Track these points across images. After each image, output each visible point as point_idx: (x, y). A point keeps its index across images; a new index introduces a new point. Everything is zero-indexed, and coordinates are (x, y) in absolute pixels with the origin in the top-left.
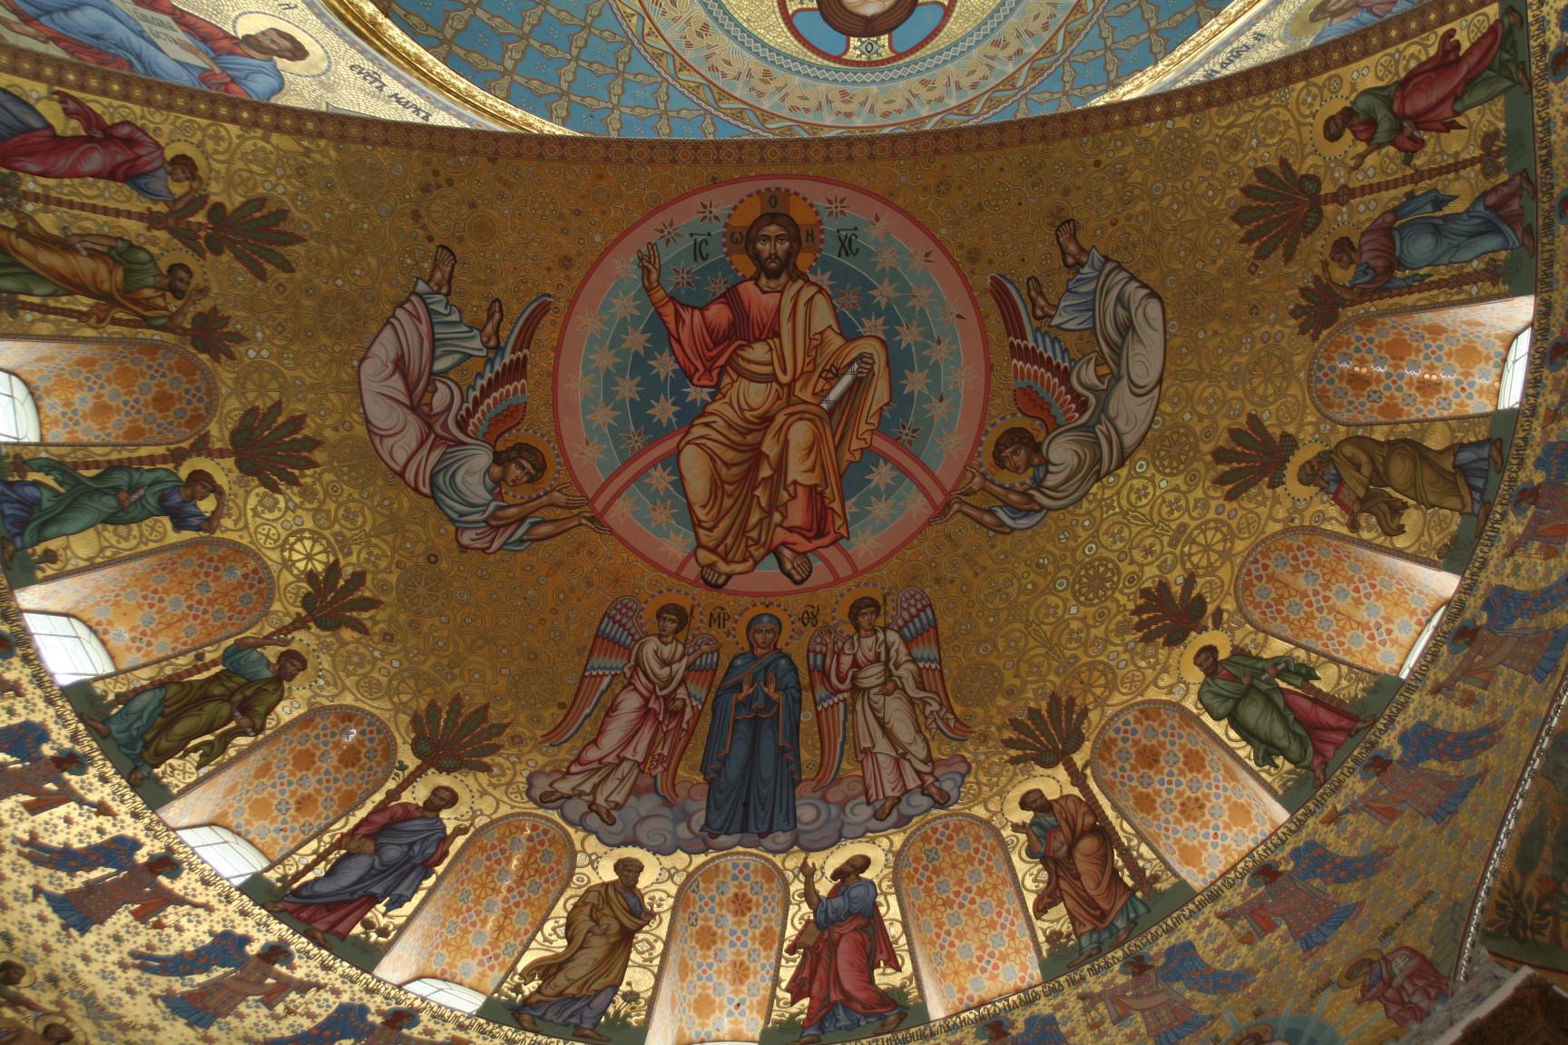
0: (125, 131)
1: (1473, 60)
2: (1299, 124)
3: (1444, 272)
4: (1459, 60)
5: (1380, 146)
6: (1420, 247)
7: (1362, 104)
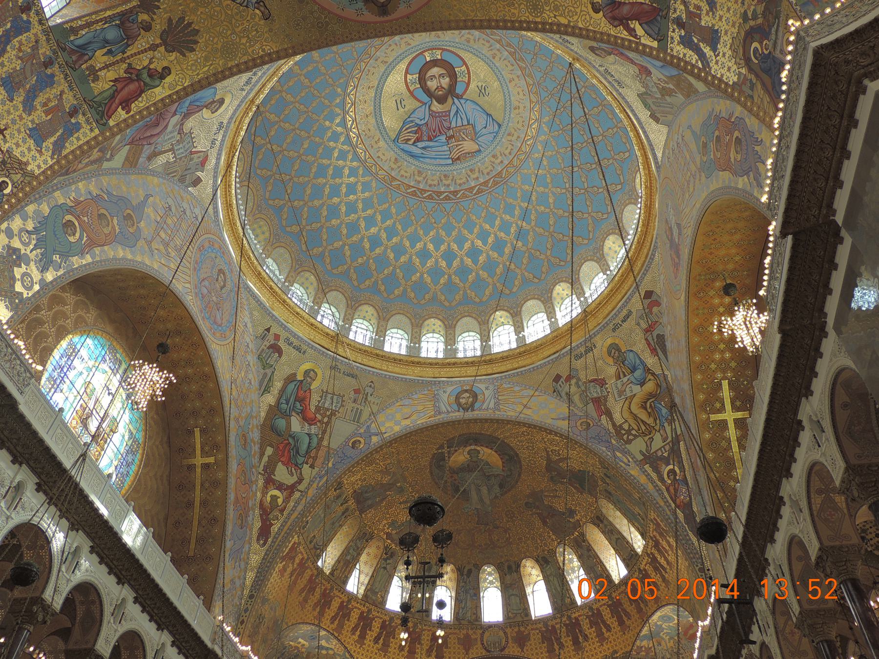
0: (616, 23)
1: (114, 106)
2: (182, 70)
3: (98, 27)
4: (121, 104)
5: (144, 68)
6: (112, 34)
7: (157, 82)
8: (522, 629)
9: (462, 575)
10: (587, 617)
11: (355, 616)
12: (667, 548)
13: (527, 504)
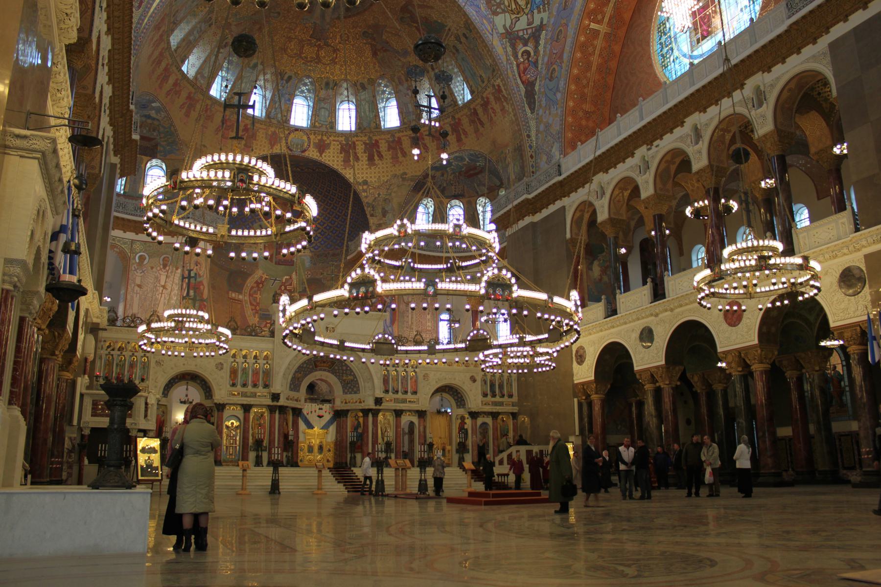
8: (325, 138)
9: (282, 79)
10: (387, 142)
11: (184, 94)
12: (498, 110)
13: (364, 33)
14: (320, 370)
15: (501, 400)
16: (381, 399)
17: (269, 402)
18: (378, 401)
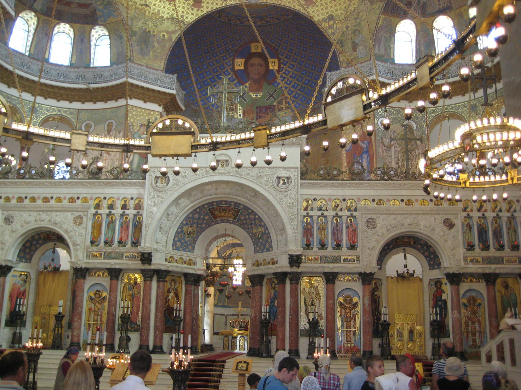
14: (222, 222)
15: (499, 254)
16: (299, 257)
17: (138, 264)
18: (295, 260)
